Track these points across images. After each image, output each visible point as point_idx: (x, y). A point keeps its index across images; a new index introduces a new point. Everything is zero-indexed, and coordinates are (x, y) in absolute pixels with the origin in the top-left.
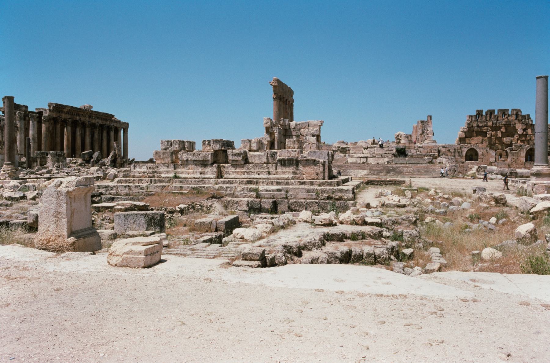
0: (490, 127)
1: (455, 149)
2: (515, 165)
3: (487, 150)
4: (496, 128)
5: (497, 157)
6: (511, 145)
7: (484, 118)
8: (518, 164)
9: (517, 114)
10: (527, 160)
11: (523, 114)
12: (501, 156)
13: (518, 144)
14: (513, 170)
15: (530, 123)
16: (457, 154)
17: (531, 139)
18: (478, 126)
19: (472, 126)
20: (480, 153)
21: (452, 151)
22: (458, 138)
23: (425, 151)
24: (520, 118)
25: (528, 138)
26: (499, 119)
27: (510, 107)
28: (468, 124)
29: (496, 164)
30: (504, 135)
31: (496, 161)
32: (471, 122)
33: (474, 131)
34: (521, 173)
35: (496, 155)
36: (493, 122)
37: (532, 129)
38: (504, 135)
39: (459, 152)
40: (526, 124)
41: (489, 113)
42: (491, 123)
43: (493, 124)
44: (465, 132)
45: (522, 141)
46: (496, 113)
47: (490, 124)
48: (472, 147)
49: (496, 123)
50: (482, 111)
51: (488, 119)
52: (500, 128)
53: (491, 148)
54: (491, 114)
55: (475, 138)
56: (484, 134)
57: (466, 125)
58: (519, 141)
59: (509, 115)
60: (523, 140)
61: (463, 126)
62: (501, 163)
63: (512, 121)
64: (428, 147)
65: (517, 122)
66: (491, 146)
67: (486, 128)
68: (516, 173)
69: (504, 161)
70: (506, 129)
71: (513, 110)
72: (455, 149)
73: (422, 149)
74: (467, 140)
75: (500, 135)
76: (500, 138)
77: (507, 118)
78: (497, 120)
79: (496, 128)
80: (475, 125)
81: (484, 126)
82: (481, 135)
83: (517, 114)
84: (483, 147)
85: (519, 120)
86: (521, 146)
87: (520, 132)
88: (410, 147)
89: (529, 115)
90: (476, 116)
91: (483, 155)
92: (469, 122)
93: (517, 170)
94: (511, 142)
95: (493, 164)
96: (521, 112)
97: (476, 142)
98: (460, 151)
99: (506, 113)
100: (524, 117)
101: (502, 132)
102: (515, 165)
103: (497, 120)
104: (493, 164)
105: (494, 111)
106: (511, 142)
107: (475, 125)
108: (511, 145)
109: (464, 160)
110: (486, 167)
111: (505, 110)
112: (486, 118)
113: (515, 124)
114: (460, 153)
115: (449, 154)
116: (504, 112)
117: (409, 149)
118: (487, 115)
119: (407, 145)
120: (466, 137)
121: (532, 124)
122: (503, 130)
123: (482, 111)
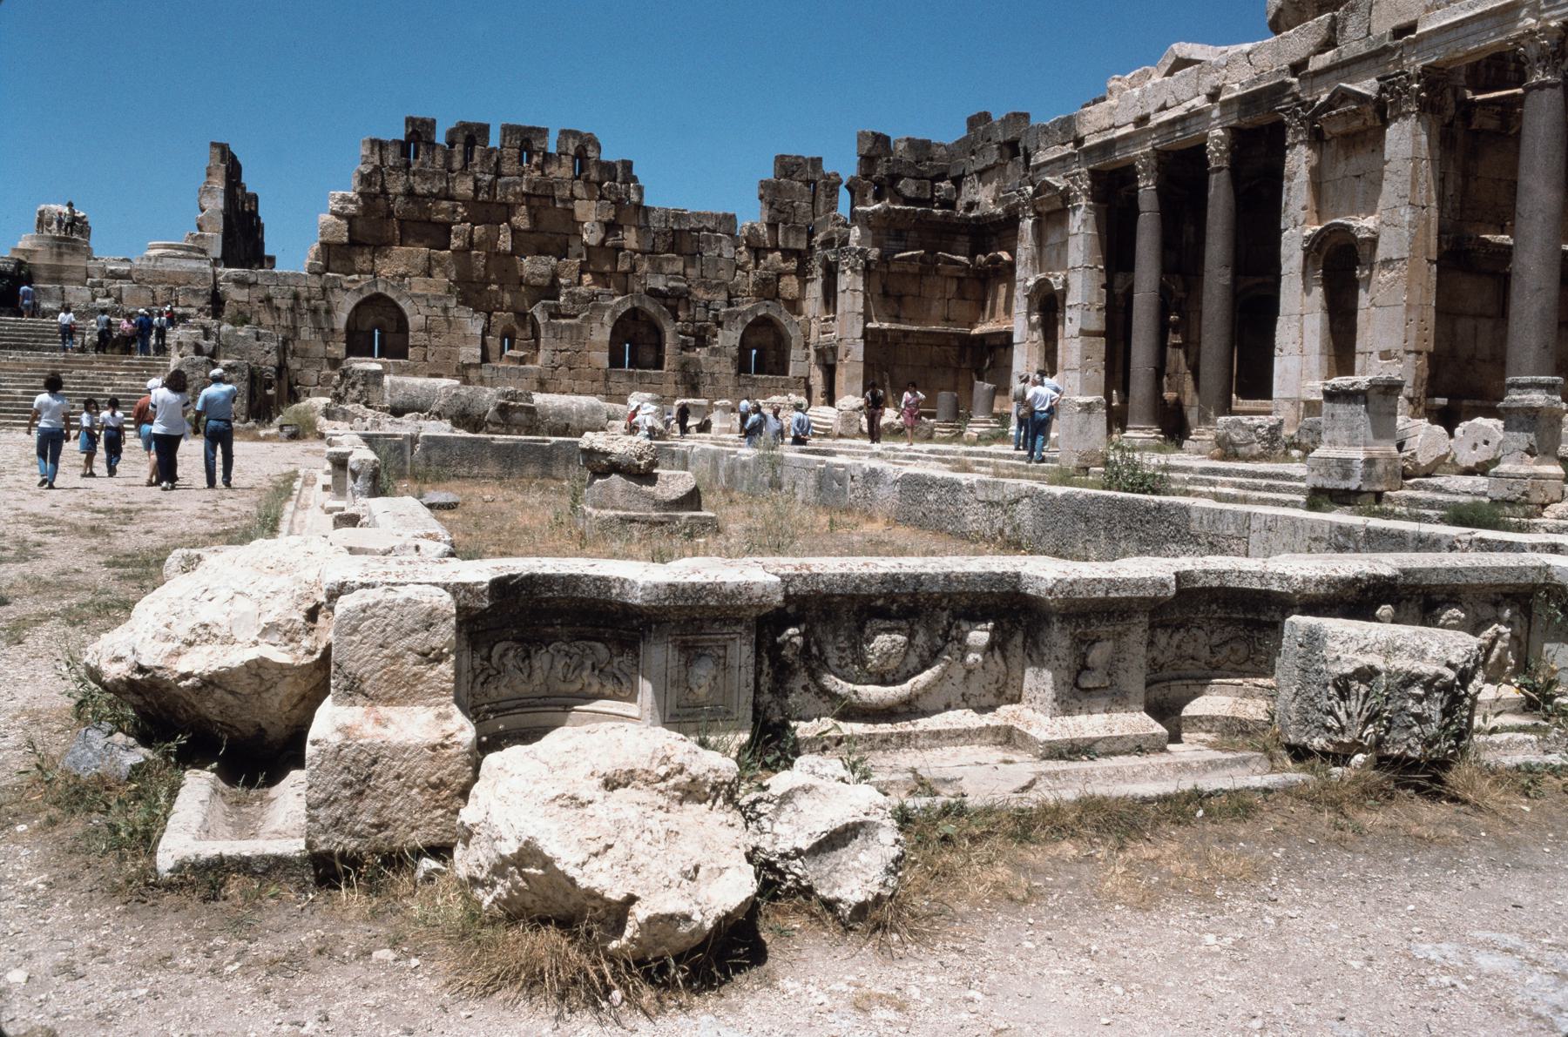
0: (465, 203)
1: (296, 297)
2: (565, 381)
3: (446, 309)
4: (488, 210)
5: (493, 342)
6: (550, 289)
7: (440, 160)
8: (577, 377)
9: (581, 156)
10: (616, 361)
11: (605, 157)
12: (509, 337)
13: (582, 290)
14: (514, 396)
15: (634, 198)
16: (308, 317)
17: (633, 269)
18: (410, 193)
19: (384, 191)
20: (415, 320)
21: (284, 303)
22: (316, 246)
23: (145, 295)
24: (594, 175)
25: (623, 266)
26: (505, 168)
27: (554, 119)
28: (365, 179)
29: (486, 372)
30: (524, 243)
31: (485, 358)
32: (377, 169)
33: (390, 213)
34: (559, 413)
35: (486, 331)
36: (476, 181)
37: (639, 228)
38: (524, 243)
39: (315, 311)
40: (619, 203)
41: (460, 138)
42: (471, 184)
43: (477, 190)
44: (350, 219)
45: (600, 277)
46: (494, 141)
47: (464, 187)
48: (381, 288)
49: (492, 186)
50: (430, 125)
51: (457, 165)
52: (508, 210)
53: (465, 301)
54: (470, 142)
55: (397, 250)
56: (438, 235)
57: (355, 182)
58: (587, 278)
59: (547, 157)
60: (603, 274)
61: (344, 190)
62: (508, 371)
63: (561, 182)
64: (161, 278)
65: (579, 190)
66: (470, 292)
67: (445, 204)
68: (531, 411)
69: (522, 361)
70: (534, 217)
71: (565, 133)
72: (296, 297)
73: (125, 285)
74: (361, 261)
75: (505, 242)
76: (506, 255)
77: (540, 167)
78: (498, 175)
79: (488, 210)
80: (397, 186)
81: (437, 197)
82: (420, 239)
83: (581, 156)
84: (432, 291)
85: (587, 181)
86: (595, 296)
87: (591, 236)
88: (60, 269)
89: (628, 165)
90: (404, 147)
91: (427, 330)
92: (367, 169)
93: (539, 399)
94: (555, 276)
95: (472, 373)
96: (599, 148)
97: (409, 277)
98: (323, 305)
99: (536, 145)
100: (608, 169)
101: (515, 231)
102: (565, 381)
103: (498, 175)
104: (472, 373)
105: (484, 129)
106: (555, 276)
107: (397, 186)
108: (550, 289)
109: (338, 350)
110: (378, 375)
111: (531, 129)
112: (448, 158)
113: (573, 197)
114: (321, 315)
115: (267, 318)
116: (526, 139)
117: (58, 280)
118: (452, 144)
119: (43, 259)
120: (353, 242)
121: (638, 206)
122: (521, 220)
123: (430, 125)
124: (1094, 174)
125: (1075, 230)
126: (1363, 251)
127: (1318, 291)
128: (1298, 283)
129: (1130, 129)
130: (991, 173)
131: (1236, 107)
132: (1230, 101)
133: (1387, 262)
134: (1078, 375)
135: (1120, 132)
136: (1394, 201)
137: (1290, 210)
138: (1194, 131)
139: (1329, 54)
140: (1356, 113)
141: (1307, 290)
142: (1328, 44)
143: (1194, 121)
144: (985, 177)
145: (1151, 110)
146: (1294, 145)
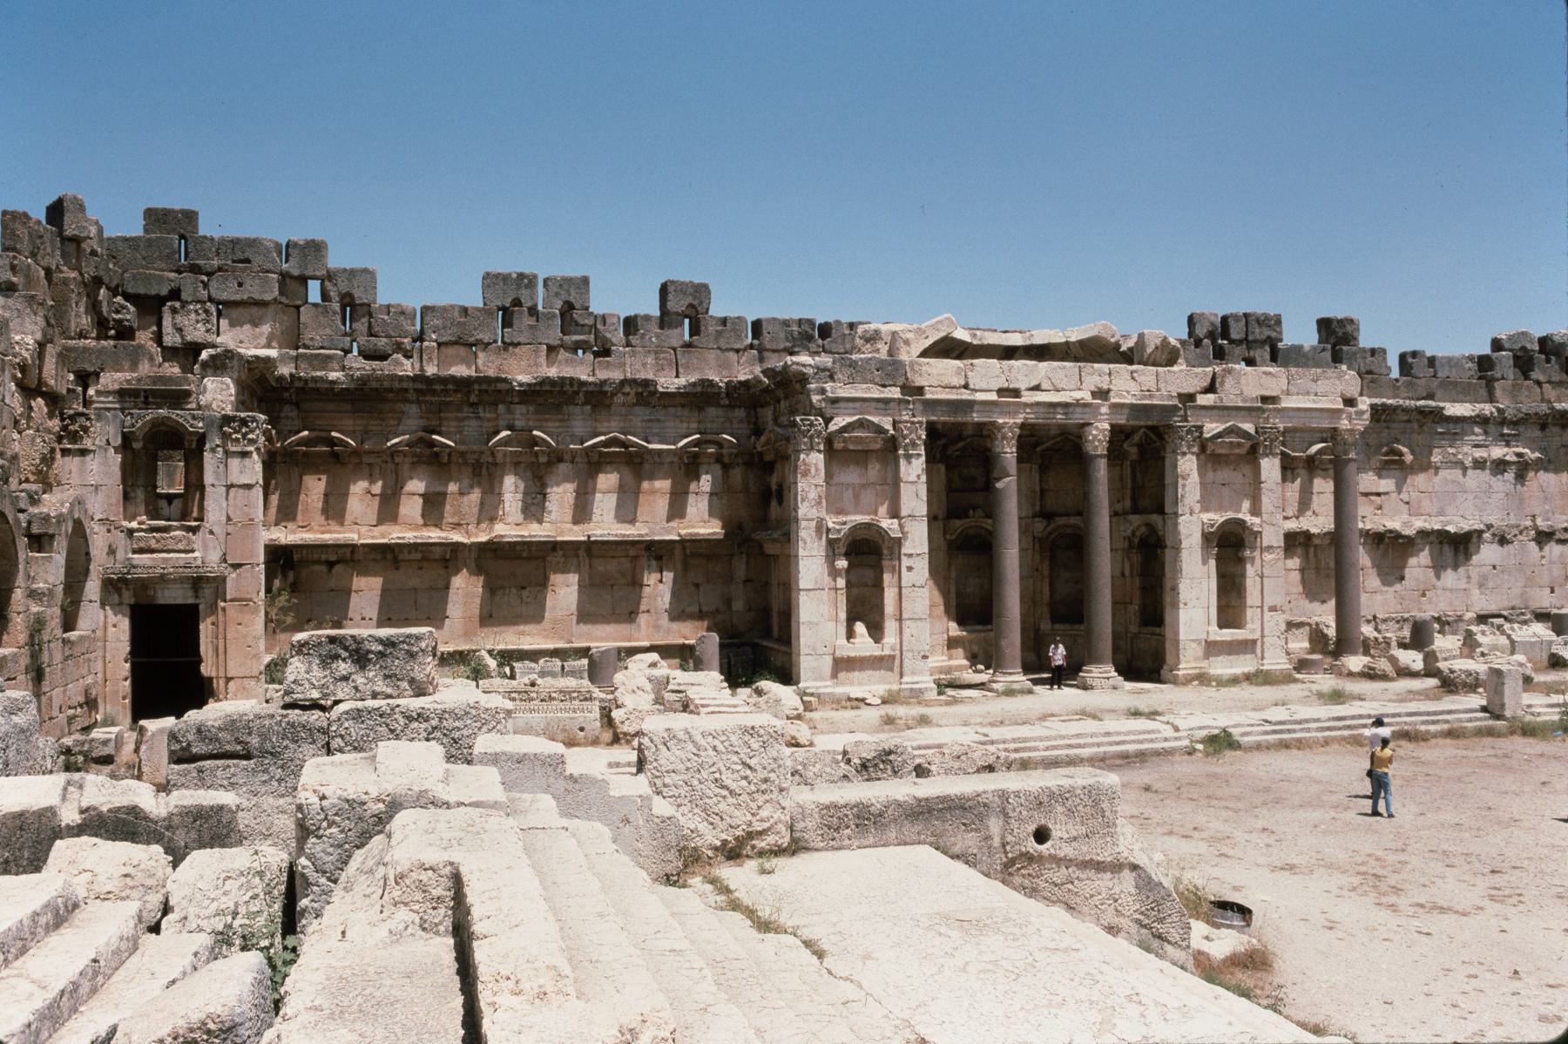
124: (932, 429)
125: (913, 478)
126: (1248, 539)
127: (1212, 563)
128: (1197, 554)
129: (993, 397)
130: (254, 310)
131: (1126, 411)
132: (1122, 405)
133: (1270, 548)
134: (927, 625)
135: (980, 396)
136: (1271, 508)
137: (1186, 501)
138: (1077, 417)
139: (1211, 396)
140: (1239, 444)
141: (1205, 562)
142: (1211, 389)
143: (1079, 410)
144: (236, 313)
145: (1022, 386)
146: (1184, 454)
